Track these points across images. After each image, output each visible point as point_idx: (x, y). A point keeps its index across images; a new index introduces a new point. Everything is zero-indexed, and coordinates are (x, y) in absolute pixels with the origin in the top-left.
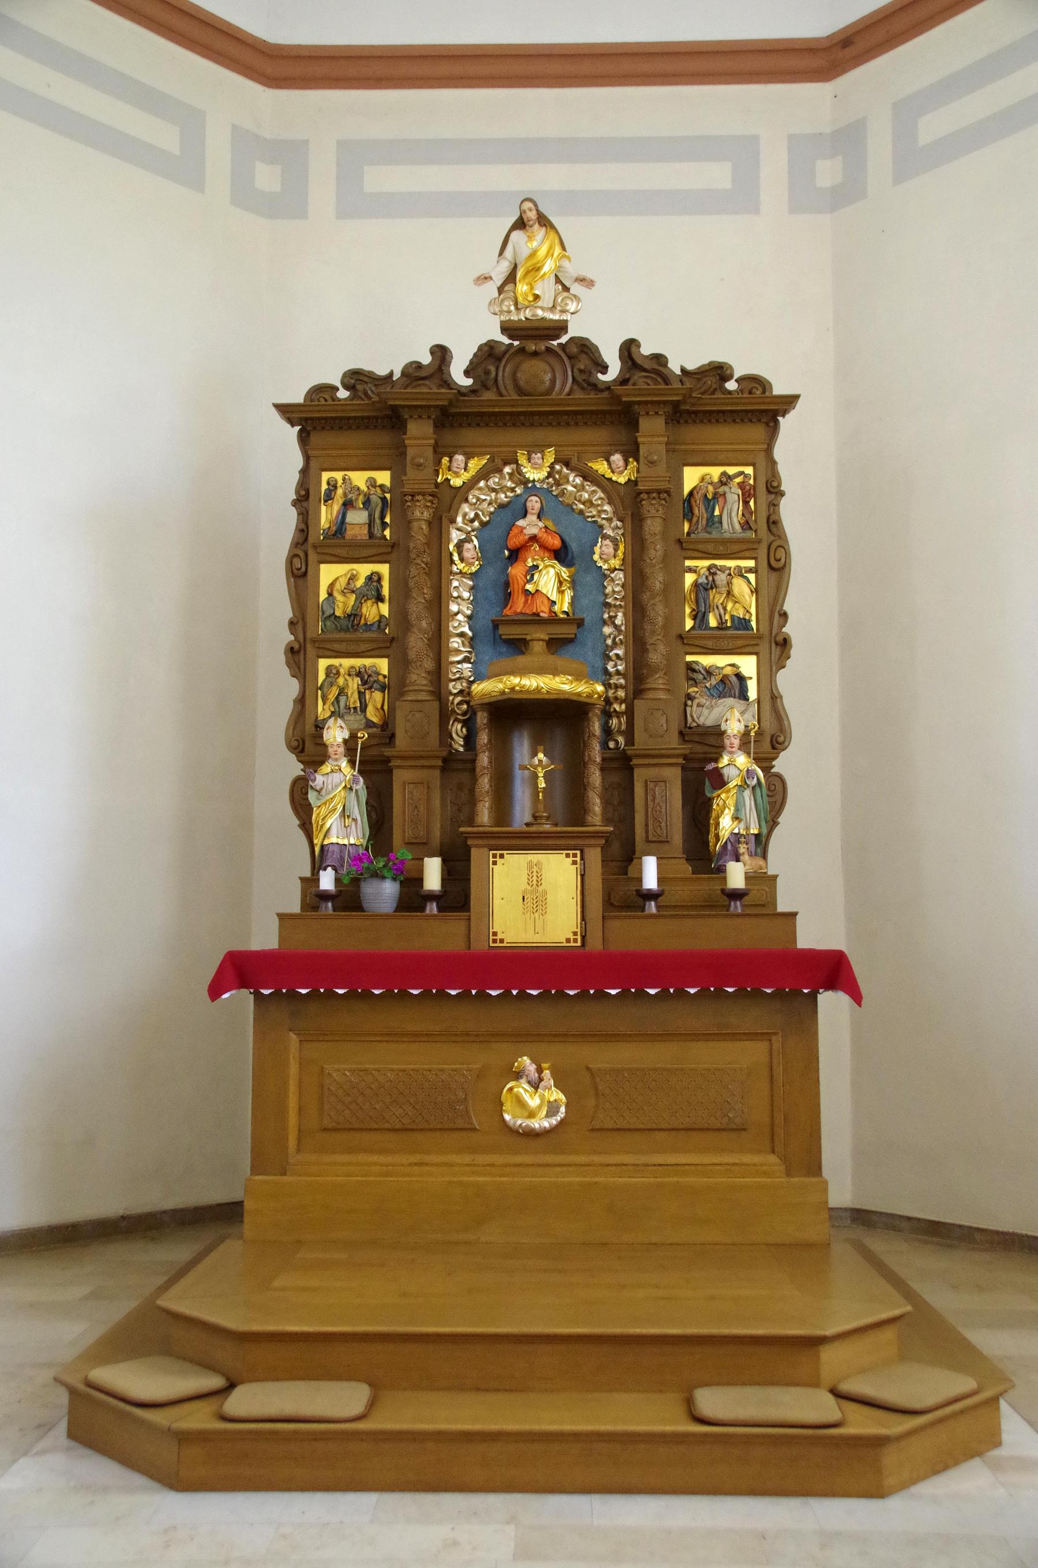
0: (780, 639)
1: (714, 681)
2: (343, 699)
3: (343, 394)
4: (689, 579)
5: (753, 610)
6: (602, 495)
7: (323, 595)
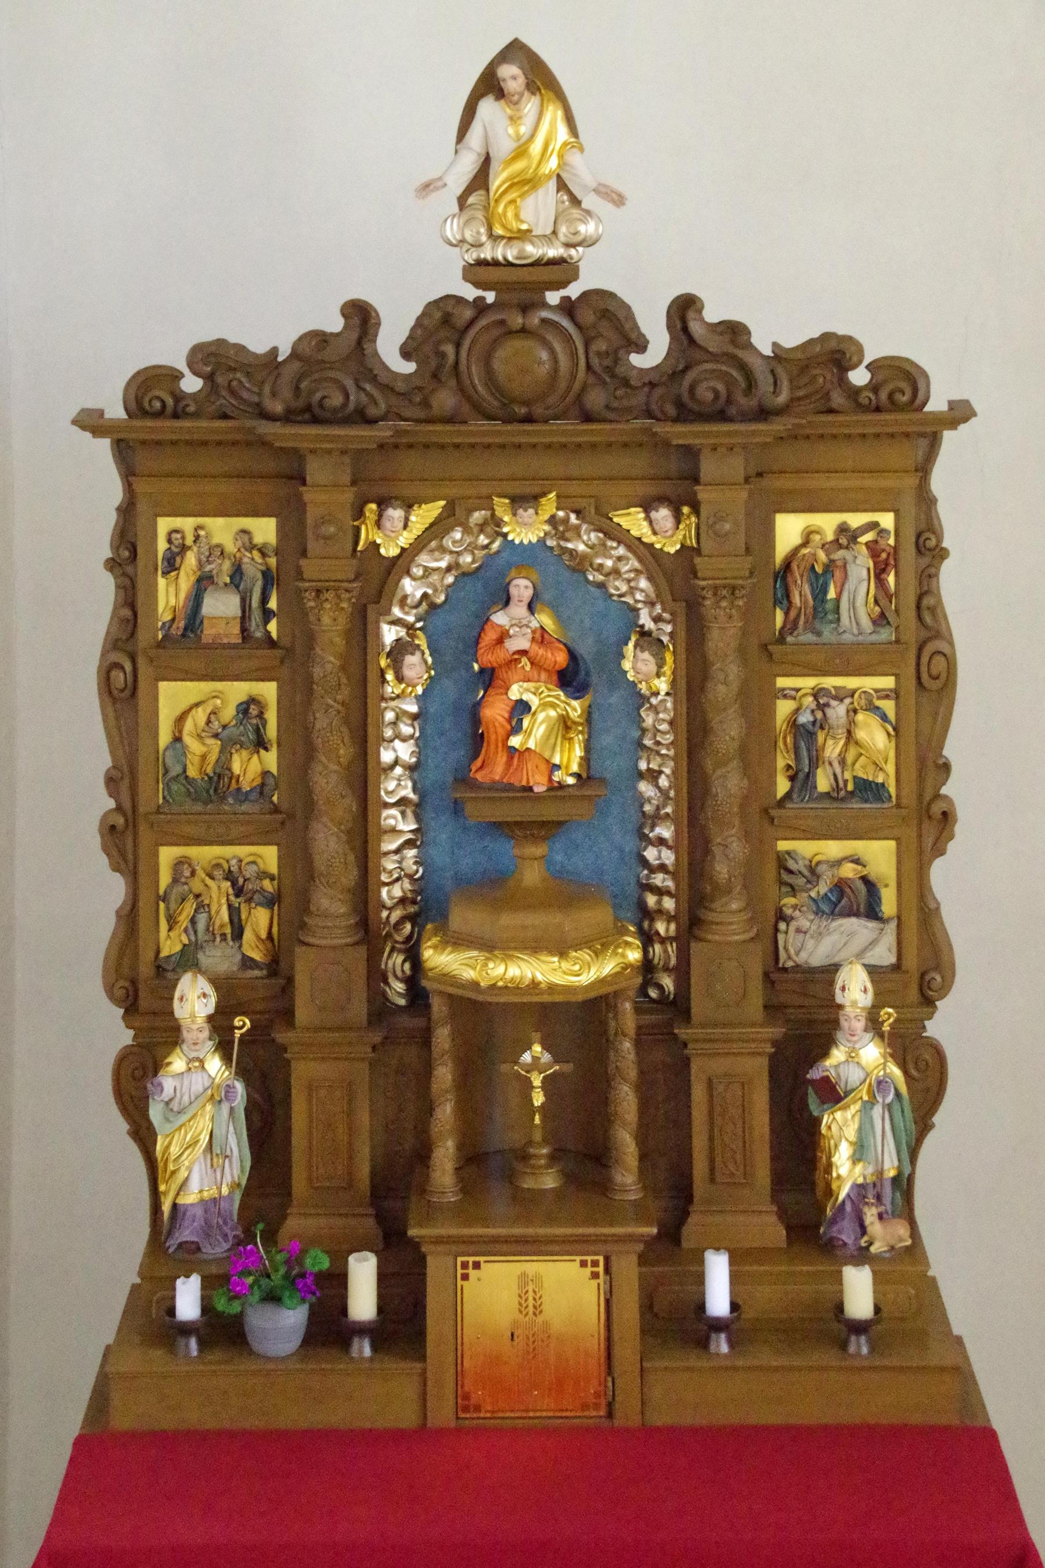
0: (937, 808)
1: (823, 888)
2: (202, 919)
3: (191, 384)
4: (784, 708)
5: (891, 768)
6: (637, 565)
7: (165, 737)
